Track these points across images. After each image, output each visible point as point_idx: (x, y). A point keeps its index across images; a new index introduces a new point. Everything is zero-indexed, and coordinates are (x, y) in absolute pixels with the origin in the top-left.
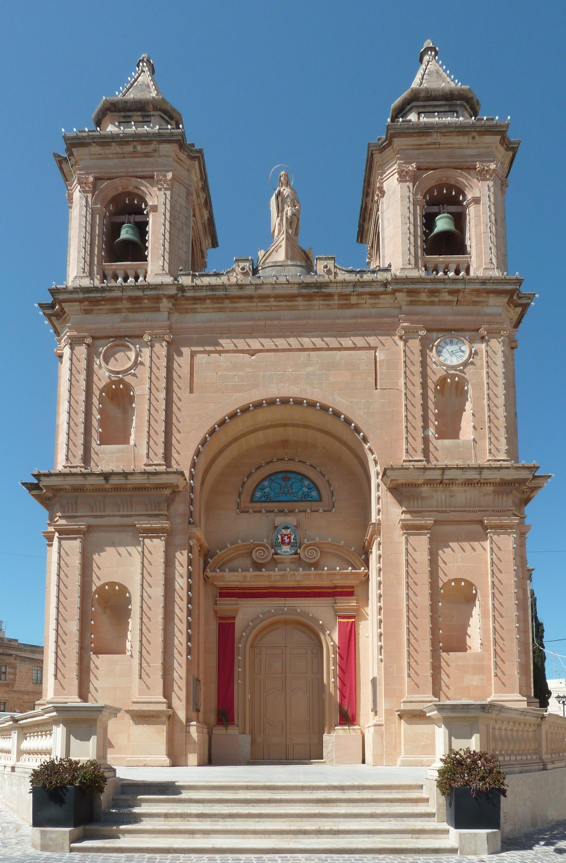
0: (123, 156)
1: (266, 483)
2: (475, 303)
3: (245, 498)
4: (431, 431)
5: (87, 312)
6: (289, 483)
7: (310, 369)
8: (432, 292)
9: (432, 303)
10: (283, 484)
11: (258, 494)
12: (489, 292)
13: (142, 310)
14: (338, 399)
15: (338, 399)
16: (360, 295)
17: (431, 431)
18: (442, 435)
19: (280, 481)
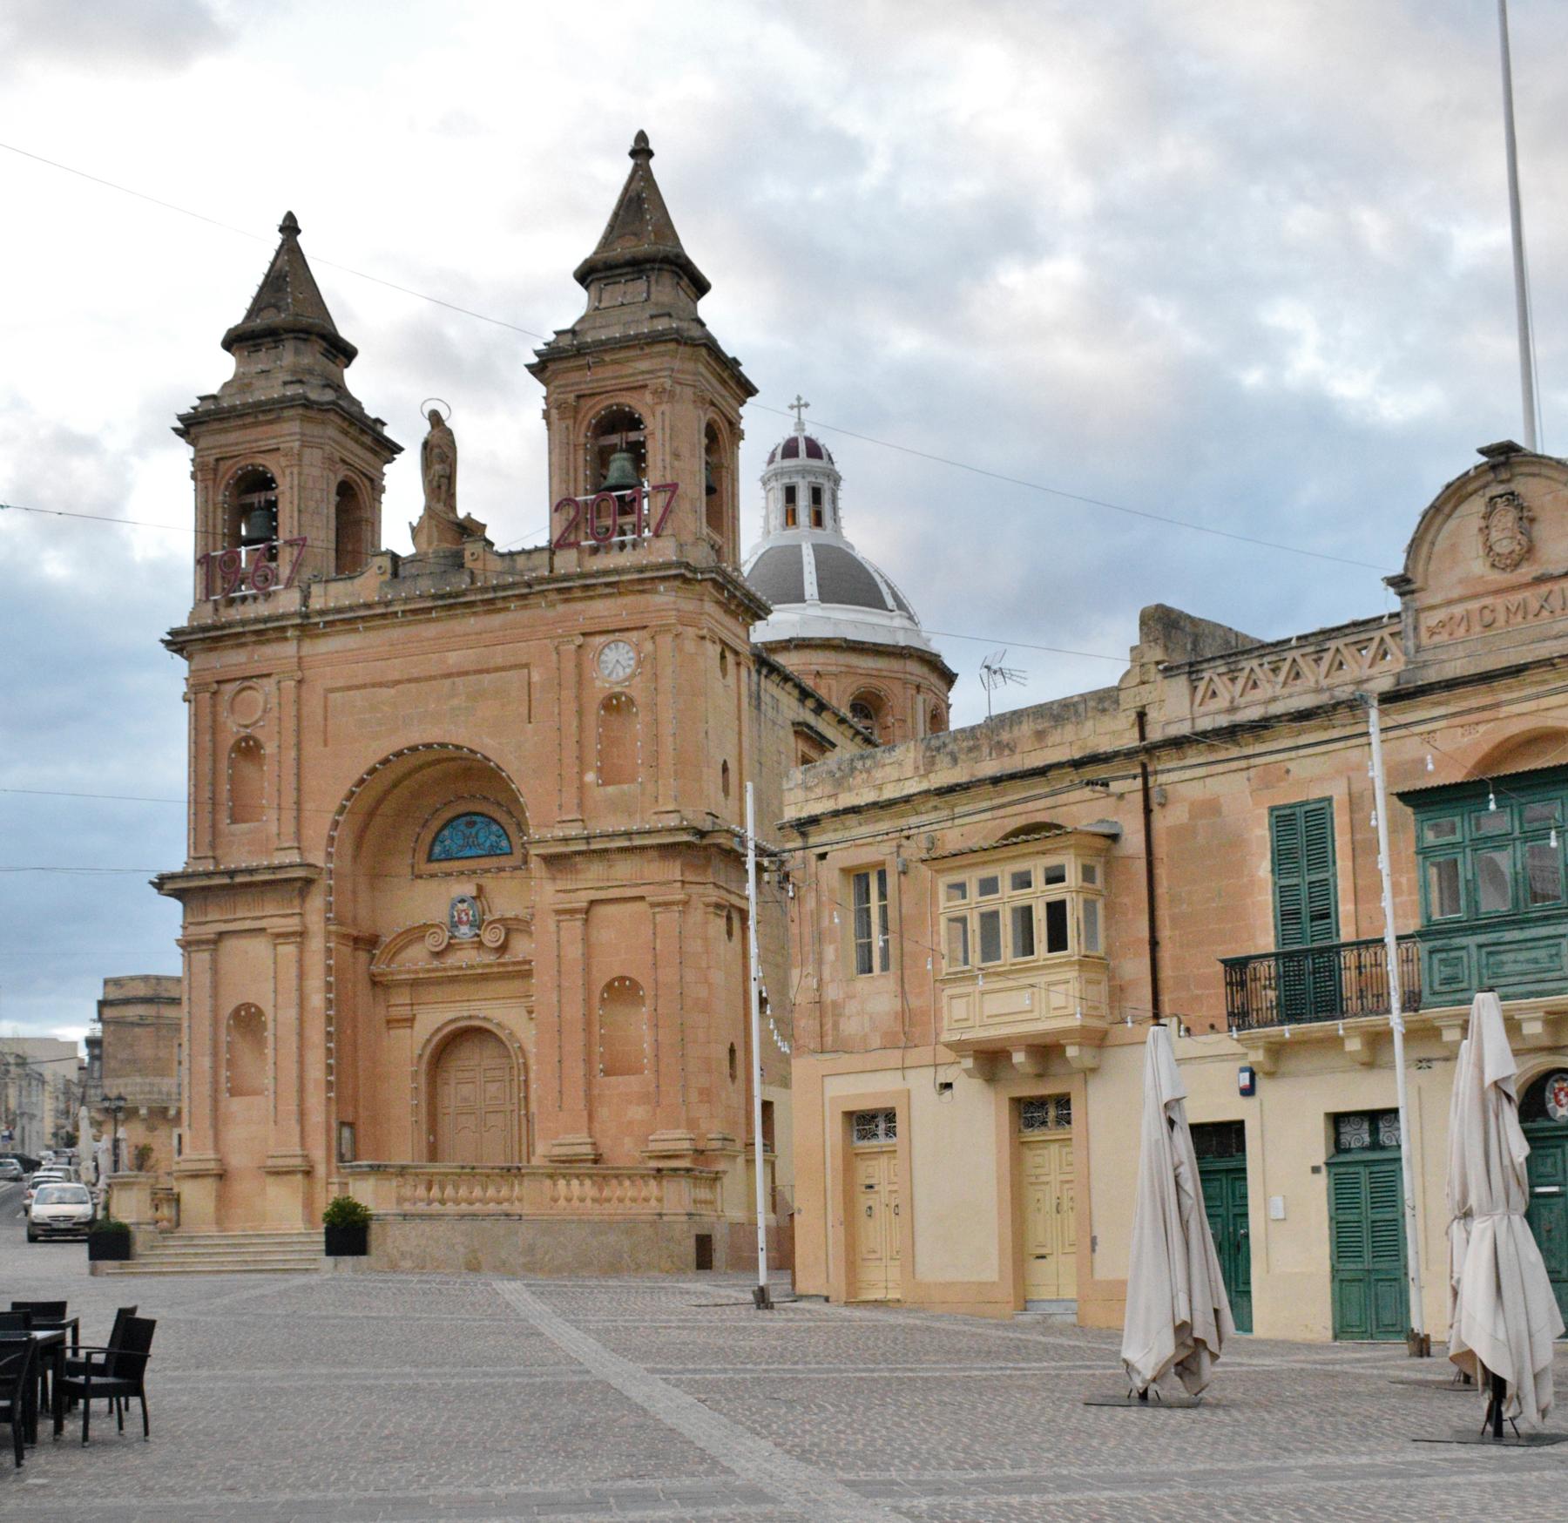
0: (244, 427)
1: (446, 832)
2: (643, 592)
3: (422, 856)
4: (590, 777)
5: (211, 650)
6: (474, 831)
7: (455, 702)
8: (586, 587)
9: (591, 598)
10: (467, 832)
11: (437, 849)
12: (652, 579)
13: (268, 641)
14: (487, 740)
15: (487, 740)
16: (504, 598)
17: (590, 777)
18: (606, 778)
19: (462, 827)
